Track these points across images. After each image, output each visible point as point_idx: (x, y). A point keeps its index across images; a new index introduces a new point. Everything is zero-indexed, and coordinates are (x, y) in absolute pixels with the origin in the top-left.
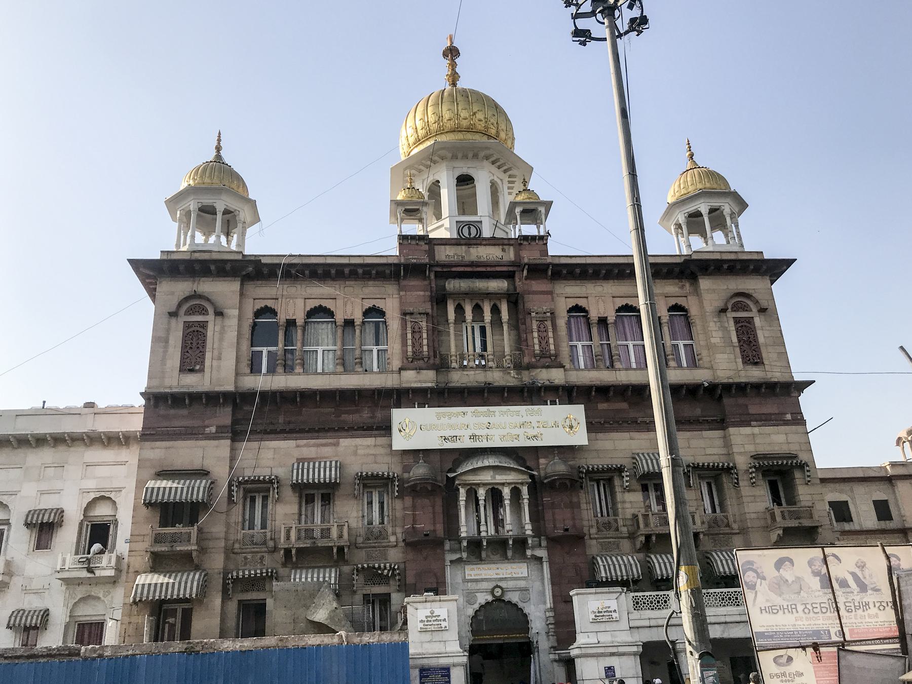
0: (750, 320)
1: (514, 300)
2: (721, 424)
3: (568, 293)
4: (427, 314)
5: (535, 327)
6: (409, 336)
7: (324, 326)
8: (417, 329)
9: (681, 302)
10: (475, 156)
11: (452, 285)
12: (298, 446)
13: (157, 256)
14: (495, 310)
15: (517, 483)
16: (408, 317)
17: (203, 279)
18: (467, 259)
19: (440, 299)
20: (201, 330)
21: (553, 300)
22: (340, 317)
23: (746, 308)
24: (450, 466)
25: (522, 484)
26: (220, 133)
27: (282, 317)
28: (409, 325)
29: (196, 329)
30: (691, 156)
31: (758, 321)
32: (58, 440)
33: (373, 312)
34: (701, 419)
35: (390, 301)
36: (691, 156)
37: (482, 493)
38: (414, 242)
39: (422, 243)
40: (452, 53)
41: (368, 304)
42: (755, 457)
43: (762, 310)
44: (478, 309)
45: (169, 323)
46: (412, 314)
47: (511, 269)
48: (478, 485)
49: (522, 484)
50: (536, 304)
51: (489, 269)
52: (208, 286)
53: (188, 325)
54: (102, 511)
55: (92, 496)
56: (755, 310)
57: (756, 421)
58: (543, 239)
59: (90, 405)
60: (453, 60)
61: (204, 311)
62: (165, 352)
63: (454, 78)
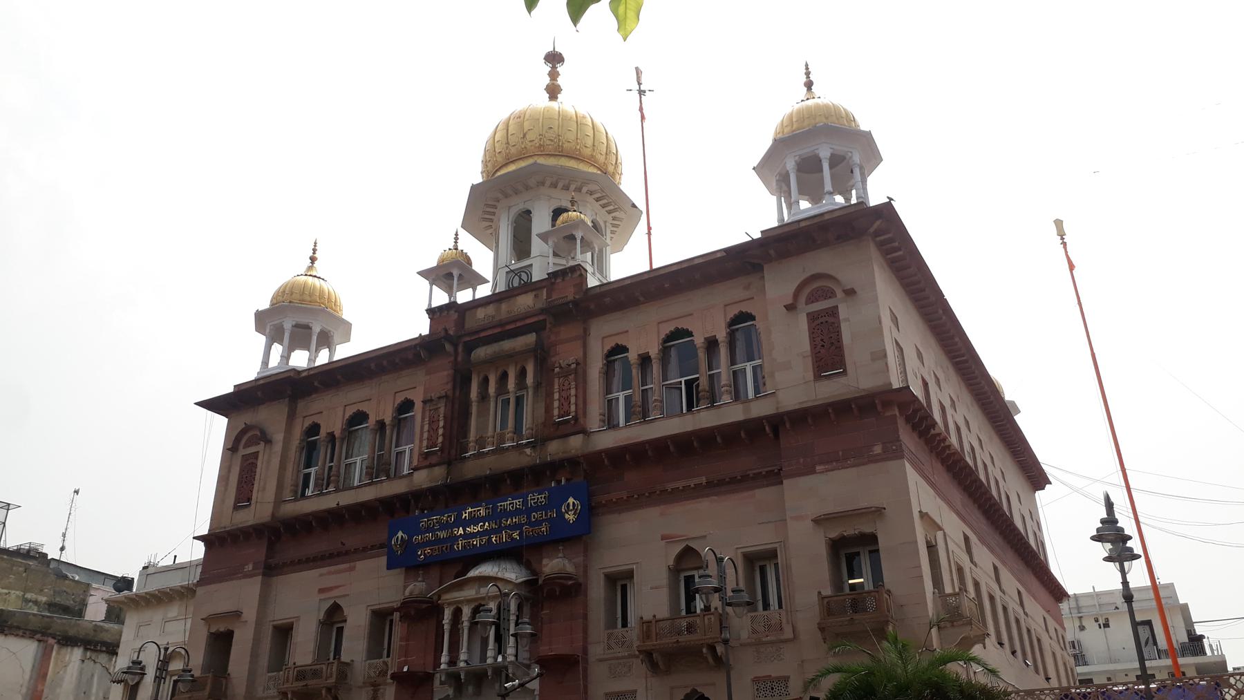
0: (833, 312)
1: (541, 355)
2: (775, 477)
3: (602, 334)
6: (426, 428)
10: (527, 188)
12: (321, 575)
13: (231, 390)
18: (497, 318)
19: (462, 379)
21: (585, 346)
31: (843, 312)
34: (751, 473)
35: (419, 386)
37: (467, 611)
40: (554, 59)
42: (817, 521)
43: (850, 292)
46: (431, 400)
47: (541, 318)
50: (566, 355)
51: (519, 324)
56: (840, 294)
57: (821, 463)
60: (554, 67)
63: (553, 91)
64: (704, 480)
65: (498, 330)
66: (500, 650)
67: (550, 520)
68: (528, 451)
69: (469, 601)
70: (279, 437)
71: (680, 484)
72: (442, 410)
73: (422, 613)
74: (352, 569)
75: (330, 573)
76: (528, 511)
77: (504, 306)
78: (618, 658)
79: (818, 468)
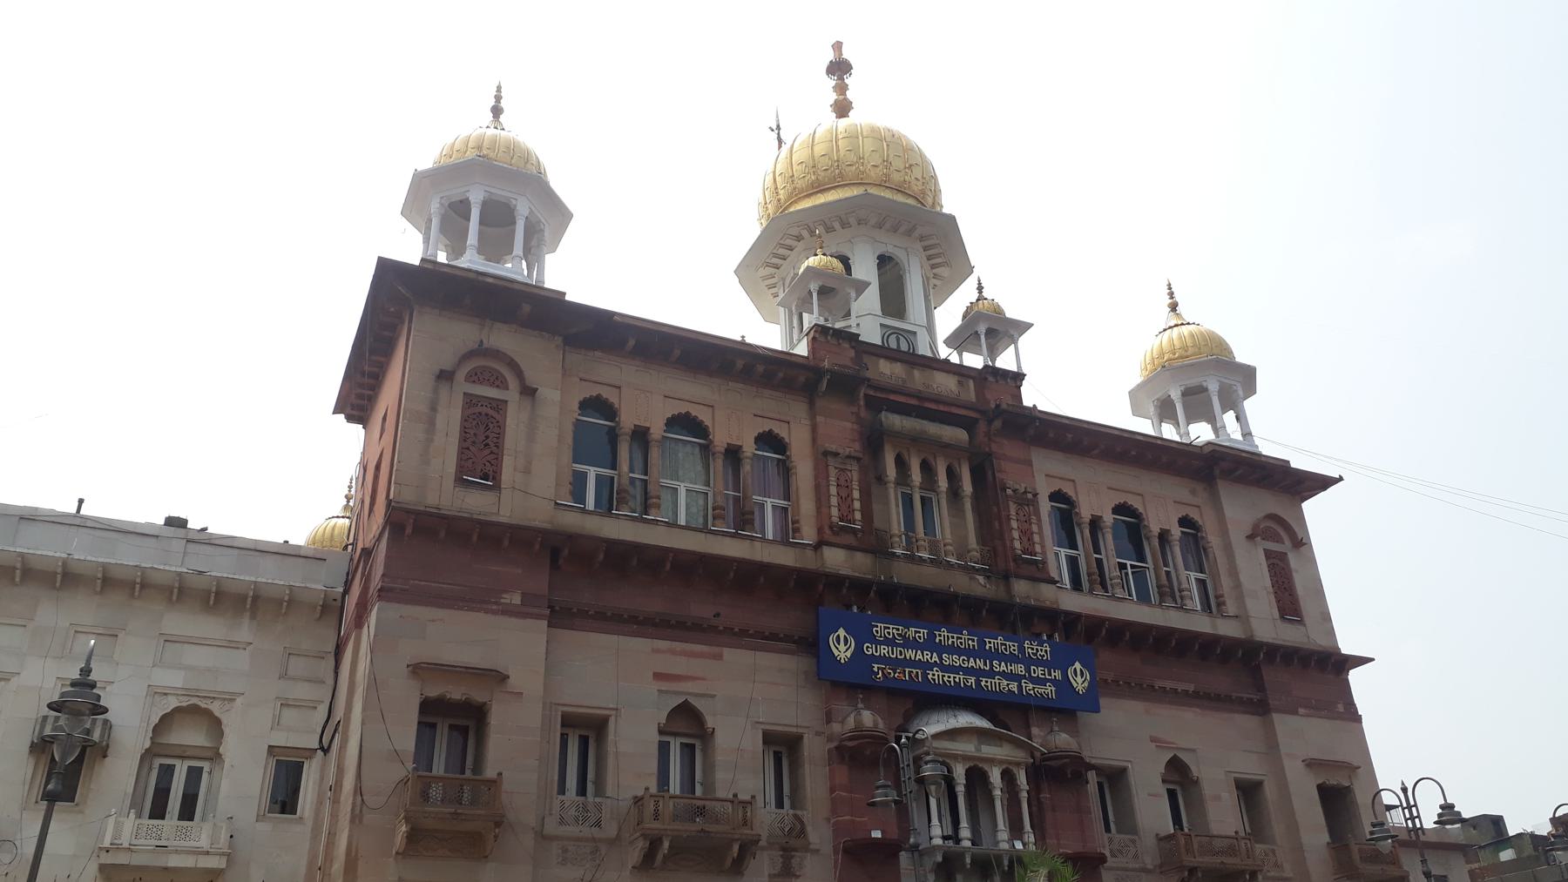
0: (1282, 556)
4: (858, 459)
5: (1013, 512)
7: (688, 448)
8: (842, 482)
9: (1194, 514)
11: (895, 421)
12: (656, 651)
13: (417, 262)
14: (952, 475)
15: (1010, 763)
16: (831, 461)
17: (499, 325)
19: (873, 441)
20: (491, 412)
22: (721, 438)
23: (1277, 539)
24: (900, 721)
25: (1018, 764)
26: (499, 89)
27: (627, 421)
28: (833, 472)
29: (484, 410)
30: (1174, 307)
31: (1293, 560)
32: (109, 582)
33: (769, 440)
36: (1174, 307)
37: (959, 772)
38: (834, 342)
39: (846, 345)
40: (839, 68)
41: (766, 426)
44: (927, 468)
45: (436, 391)
46: (836, 454)
48: (955, 757)
49: (1018, 764)
50: (1011, 476)
51: (941, 408)
52: (504, 339)
53: (470, 401)
54: (190, 736)
55: (173, 703)
58: (1019, 377)
59: (176, 523)
61: (499, 382)
62: (429, 440)
64: (1191, 688)
65: (914, 402)
66: (1016, 830)
67: (1054, 682)
68: (981, 579)
69: (965, 758)
70: (550, 394)
71: (1169, 685)
72: (856, 476)
73: (861, 756)
74: (719, 657)
75: (673, 652)
76: (1028, 662)
77: (916, 373)
78: (1126, 870)
79: (1301, 711)
